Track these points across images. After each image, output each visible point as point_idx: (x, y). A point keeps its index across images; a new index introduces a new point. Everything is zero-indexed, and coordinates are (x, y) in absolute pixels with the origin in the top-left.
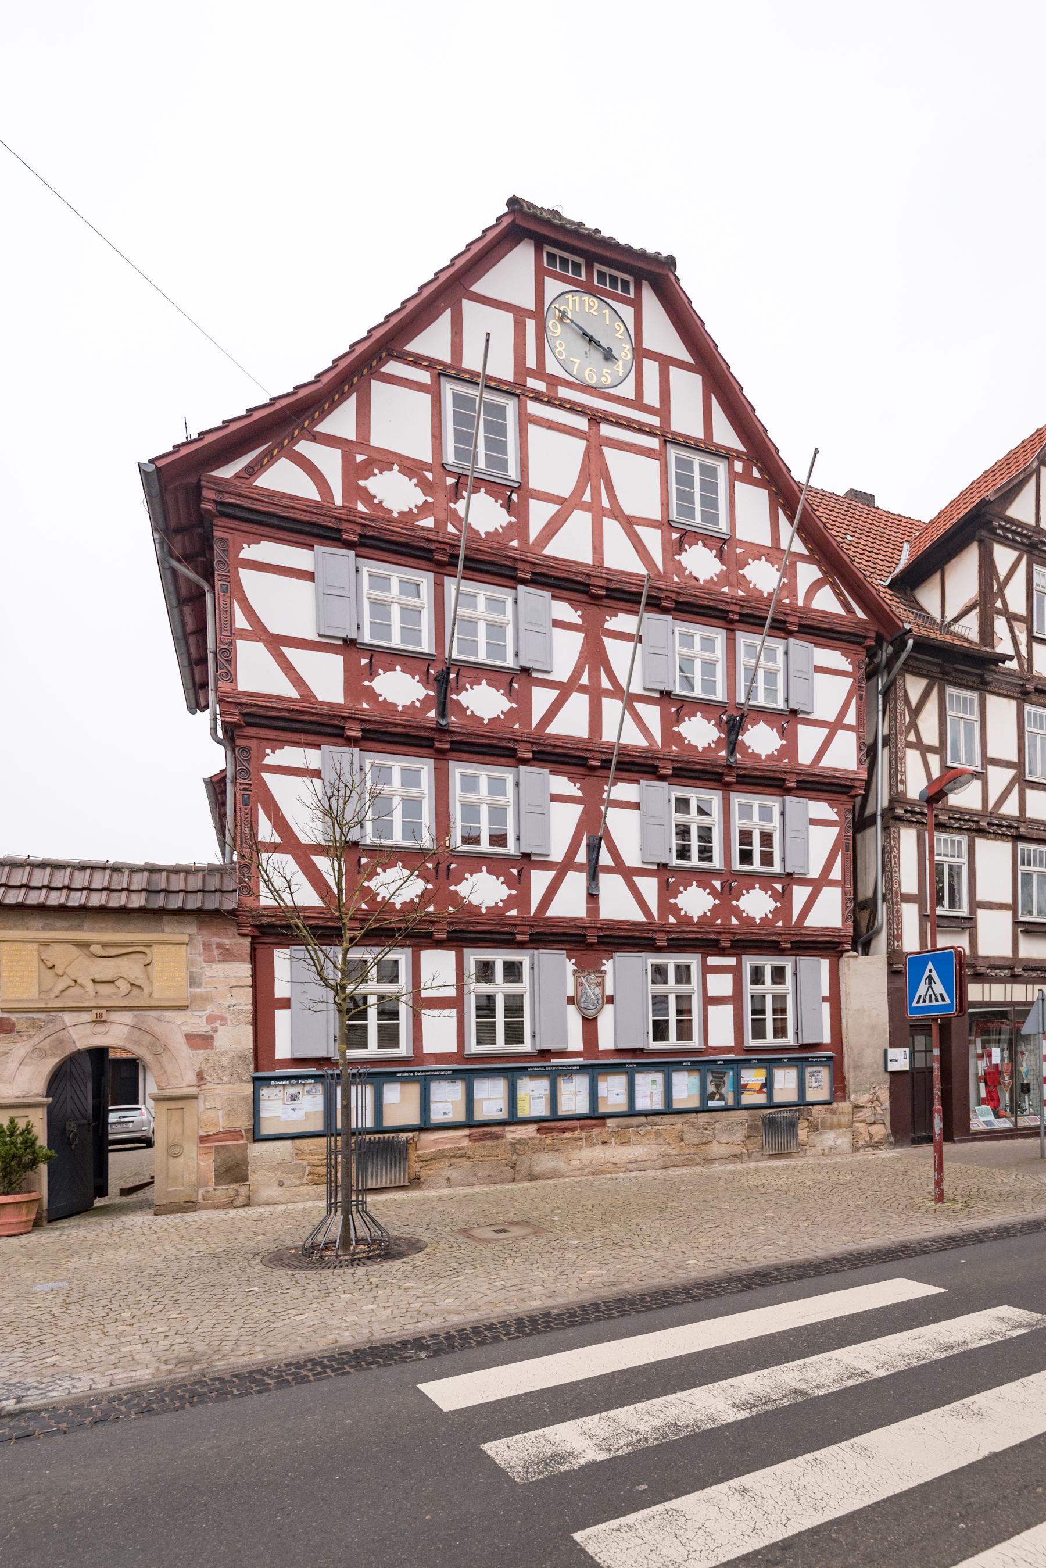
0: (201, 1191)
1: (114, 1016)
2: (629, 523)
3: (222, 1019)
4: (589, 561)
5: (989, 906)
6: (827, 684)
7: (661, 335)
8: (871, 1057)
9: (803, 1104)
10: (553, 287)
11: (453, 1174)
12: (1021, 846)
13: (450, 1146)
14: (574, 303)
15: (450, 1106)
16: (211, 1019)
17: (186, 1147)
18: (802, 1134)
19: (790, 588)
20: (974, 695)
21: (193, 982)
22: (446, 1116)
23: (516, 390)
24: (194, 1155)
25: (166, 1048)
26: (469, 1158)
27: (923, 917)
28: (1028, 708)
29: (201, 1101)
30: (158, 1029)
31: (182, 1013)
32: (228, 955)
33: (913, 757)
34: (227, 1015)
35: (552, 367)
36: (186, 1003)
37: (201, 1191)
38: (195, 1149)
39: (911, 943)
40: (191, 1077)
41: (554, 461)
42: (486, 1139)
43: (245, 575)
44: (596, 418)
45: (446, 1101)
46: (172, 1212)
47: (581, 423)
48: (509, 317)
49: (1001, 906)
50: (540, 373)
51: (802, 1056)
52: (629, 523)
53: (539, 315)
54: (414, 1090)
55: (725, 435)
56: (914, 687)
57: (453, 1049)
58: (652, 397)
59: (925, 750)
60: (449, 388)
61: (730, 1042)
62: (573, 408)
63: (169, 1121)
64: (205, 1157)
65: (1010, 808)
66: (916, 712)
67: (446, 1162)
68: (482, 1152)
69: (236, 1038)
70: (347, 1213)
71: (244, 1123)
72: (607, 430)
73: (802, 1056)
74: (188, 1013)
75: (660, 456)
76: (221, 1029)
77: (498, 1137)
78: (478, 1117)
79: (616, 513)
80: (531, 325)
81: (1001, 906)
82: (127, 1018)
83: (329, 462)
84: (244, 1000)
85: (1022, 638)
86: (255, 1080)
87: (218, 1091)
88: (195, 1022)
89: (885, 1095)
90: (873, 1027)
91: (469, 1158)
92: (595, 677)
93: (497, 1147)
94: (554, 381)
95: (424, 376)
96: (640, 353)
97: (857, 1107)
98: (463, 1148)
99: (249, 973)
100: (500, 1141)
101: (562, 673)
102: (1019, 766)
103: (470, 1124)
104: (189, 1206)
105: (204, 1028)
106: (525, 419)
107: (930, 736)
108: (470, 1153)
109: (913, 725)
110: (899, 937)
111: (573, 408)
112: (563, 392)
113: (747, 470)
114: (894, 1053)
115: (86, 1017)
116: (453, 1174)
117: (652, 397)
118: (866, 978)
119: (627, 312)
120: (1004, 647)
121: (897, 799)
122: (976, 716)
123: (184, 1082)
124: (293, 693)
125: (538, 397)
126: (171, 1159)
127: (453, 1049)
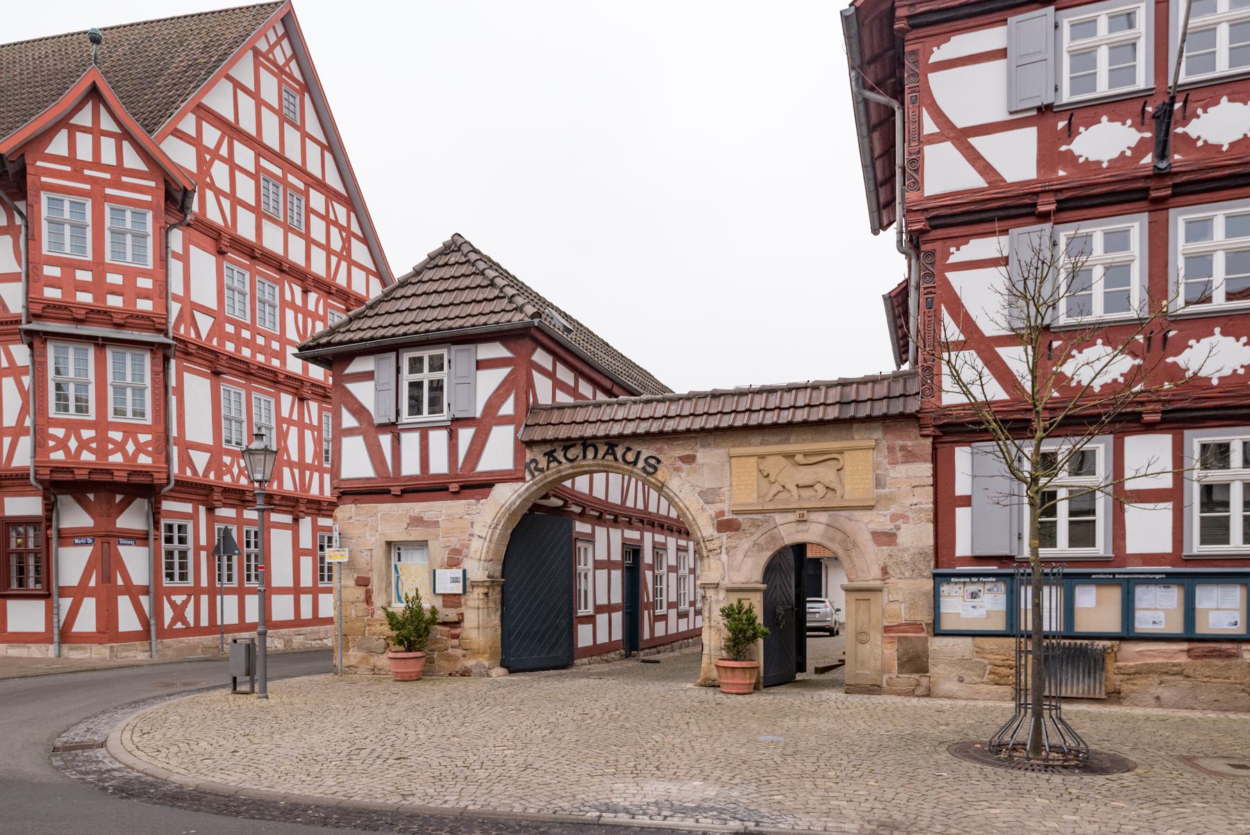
0: (885, 677)
1: (813, 516)
3: (905, 517)
11: (1166, 694)
13: (1160, 660)
15: (1162, 615)
17: (872, 634)
22: (1156, 626)
24: (879, 643)
25: (855, 545)
26: (1187, 676)
29: (885, 594)
30: (848, 526)
31: (869, 512)
34: (909, 514)
36: (872, 503)
37: (885, 677)
38: (880, 637)
42: (1213, 657)
45: (1156, 609)
46: (860, 693)
54: (1114, 595)
63: (857, 610)
64: (889, 646)
67: (1155, 679)
68: (1207, 671)
69: (917, 535)
70: (1038, 716)
74: (874, 512)
76: (903, 526)
77: (1229, 656)
78: (1201, 629)
82: (823, 517)
84: (925, 499)
86: (935, 576)
87: (900, 586)
88: (879, 520)
91: (1187, 676)
93: (1228, 667)
98: (1179, 665)
99: (930, 472)
100: (1233, 661)
104: (873, 689)
105: (889, 527)
108: (1188, 671)
115: (792, 517)
116: (1166, 694)
123: (871, 577)
126: (860, 646)
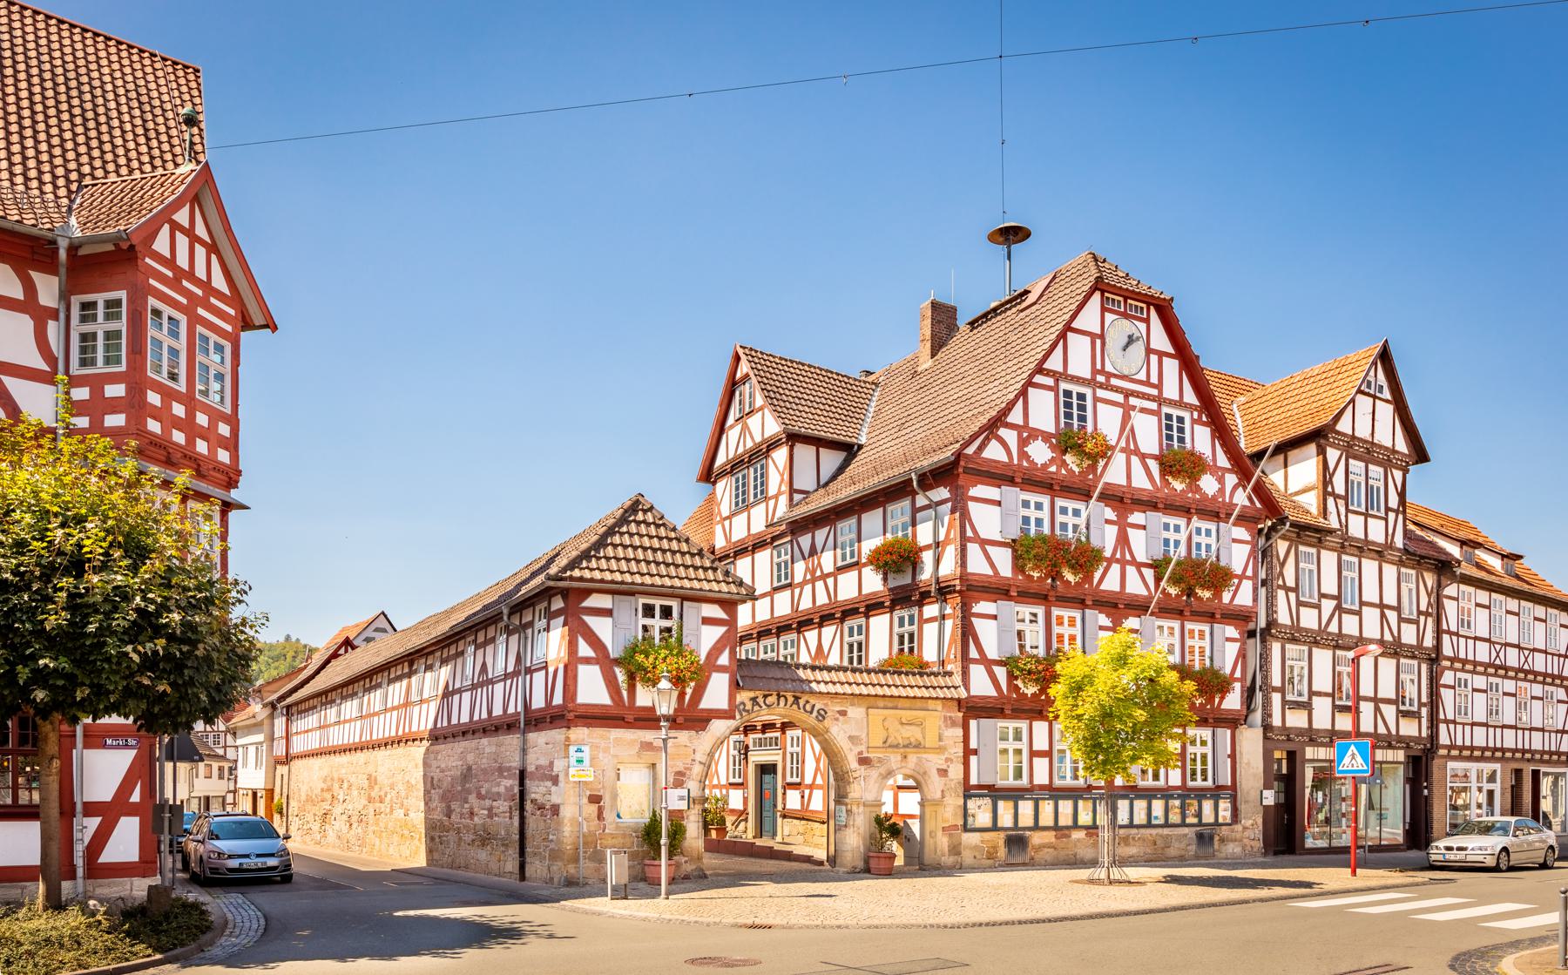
2: (1143, 457)
4: (1124, 483)
5: (1319, 694)
6: (1235, 549)
7: (1160, 340)
8: (1254, 795)
9: (1216, 824)
10: (1109, 317)
12: (1339, 652)
14: (1119, 329)
16: (947, 760)
18: (1216, 843)
19: (1222, 490)
20: (1313, 551)
21: (940, 739)
23: (1091, 383)
27: (1284, 702)
28: (1344, 557)
32: (954, 724)
33: (1281, 594)
35: (1109, 368)
39: (1276, 721)
40: (939, 795)
41: (1107, 421)
43: (971, 504)
44: (1128, 394)
47: (1119, 398)
48: (1088, 339)
49: (1326, 695)
50: (1102, 372)
51: (1216, 793)
52: (1143, 457)
53: (1102, 336)
55: (1190, 397)
56: (1282, 547)
57: (1047, 782)
58: (1154, 379)
59: (1287, 589)
60: (1063, 386)
61: (1178, 783)
62: (1117, 390)
65: (1333, 628)
66: (1283, 565)
69: (956, 772)
71: (961, 822)
72: (1133, 401)
73: (1216, 793)
75: (1157, 413)
79: (1137, 452)
80: (1098, 342)
81: (1326, 695)
83: (1010, 436)
84: (960, 750)
85: (1342, 510)
89: (1260, 821)
90: (1255, 775)
92: (1123, 554)
94: (1109, 375)
95: (1050, 381)
96: (1149, 351)
97: (1245, 828)
101: (1108, 554)
102: (1338, 598)
103: (1056, 827)
106: (1096, 399)
107: (1291, 583)
109: (1281, 574)
110: (1270, 716)
111: (1117, 390)
112: (1114, 381)
113: (1200, 417)
114: (1266, 793)
117: (1154, 379)
118: (1251, 741)
119: (1142, 326)
120: (1333, 523)
121: (1272, 623)
122: (1314, 567)
124: (991, 573)
125: (1101, 386)
127: (1047, 782)
